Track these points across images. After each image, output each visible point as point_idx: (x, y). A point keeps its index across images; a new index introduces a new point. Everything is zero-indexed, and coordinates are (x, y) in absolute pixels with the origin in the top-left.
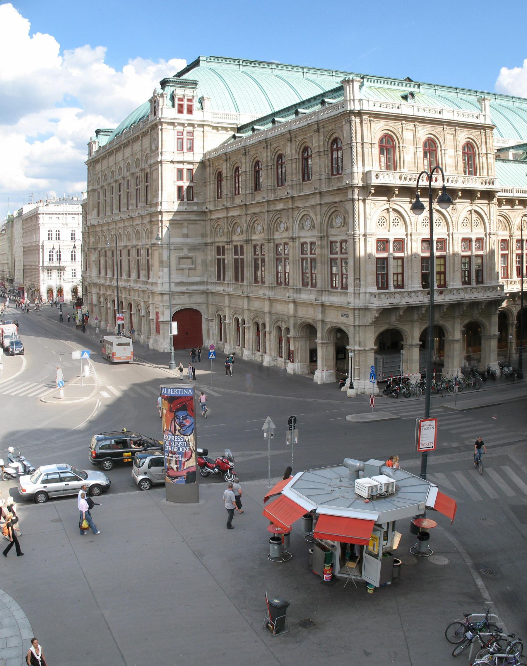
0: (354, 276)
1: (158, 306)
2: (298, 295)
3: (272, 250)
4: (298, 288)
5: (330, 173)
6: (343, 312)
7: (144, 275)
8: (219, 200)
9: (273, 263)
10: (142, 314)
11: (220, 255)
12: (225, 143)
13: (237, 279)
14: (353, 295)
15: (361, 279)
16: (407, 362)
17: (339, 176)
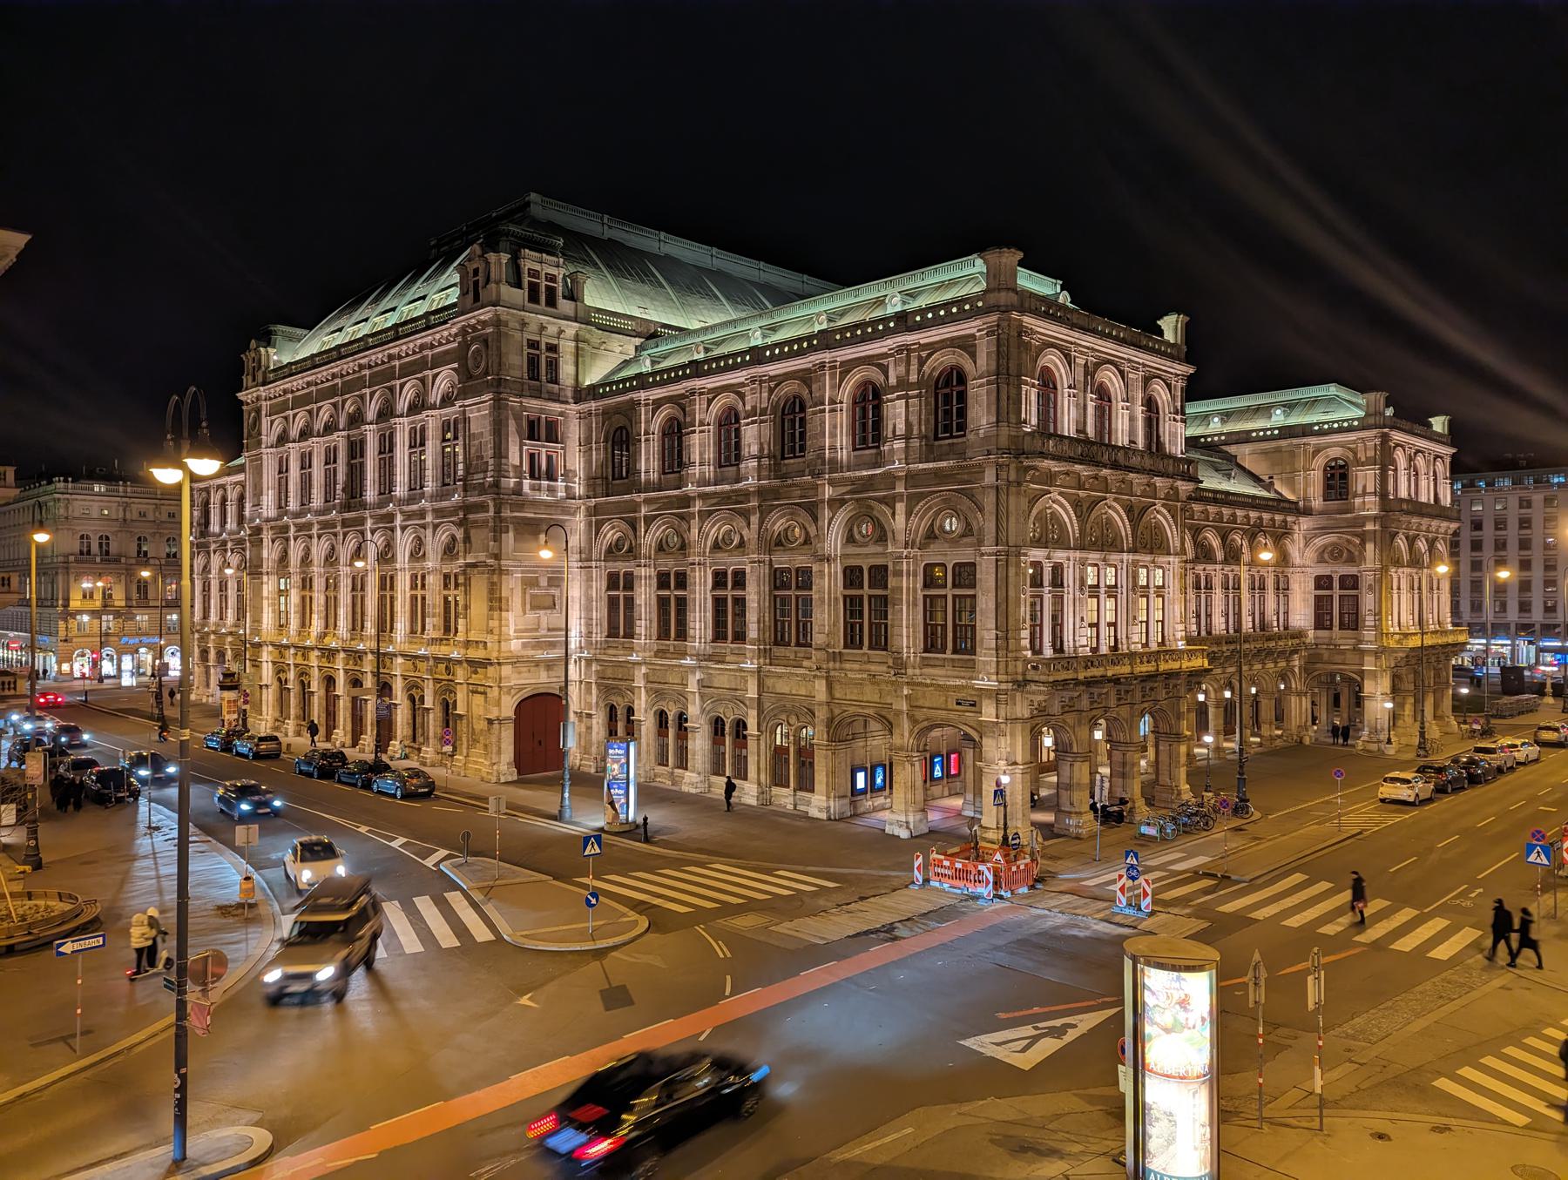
0: (997, 629)
1: (481, 689)
2: (837, 665)
3: (767, 579)
4: (837, 651)
5: (931, 435)
6: (961, 695)
7: (434, 626)
8: (618, 482)
9: (767, 604)
10: (428, 704)
11: (618, 589)
12: (613, 372)
13: (663, 634)
14: (994, 665)
15: (1009, 635)
16: (1066, 790)
17: (955, 441)
